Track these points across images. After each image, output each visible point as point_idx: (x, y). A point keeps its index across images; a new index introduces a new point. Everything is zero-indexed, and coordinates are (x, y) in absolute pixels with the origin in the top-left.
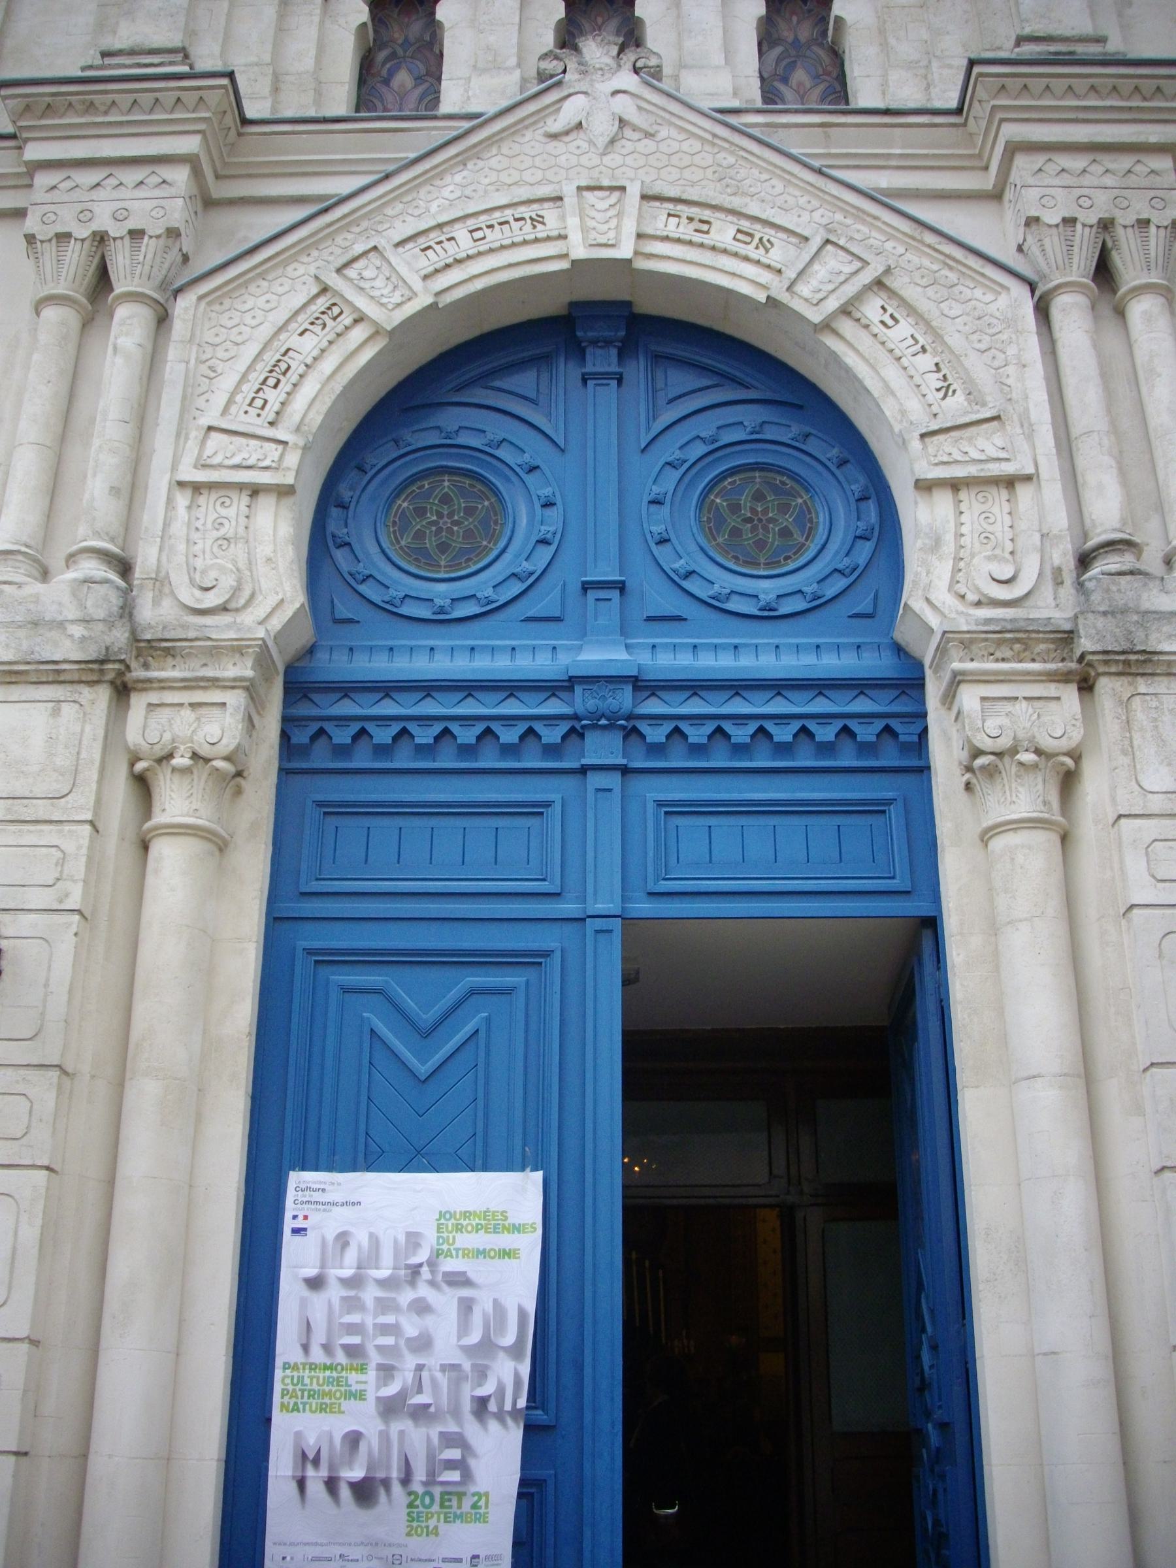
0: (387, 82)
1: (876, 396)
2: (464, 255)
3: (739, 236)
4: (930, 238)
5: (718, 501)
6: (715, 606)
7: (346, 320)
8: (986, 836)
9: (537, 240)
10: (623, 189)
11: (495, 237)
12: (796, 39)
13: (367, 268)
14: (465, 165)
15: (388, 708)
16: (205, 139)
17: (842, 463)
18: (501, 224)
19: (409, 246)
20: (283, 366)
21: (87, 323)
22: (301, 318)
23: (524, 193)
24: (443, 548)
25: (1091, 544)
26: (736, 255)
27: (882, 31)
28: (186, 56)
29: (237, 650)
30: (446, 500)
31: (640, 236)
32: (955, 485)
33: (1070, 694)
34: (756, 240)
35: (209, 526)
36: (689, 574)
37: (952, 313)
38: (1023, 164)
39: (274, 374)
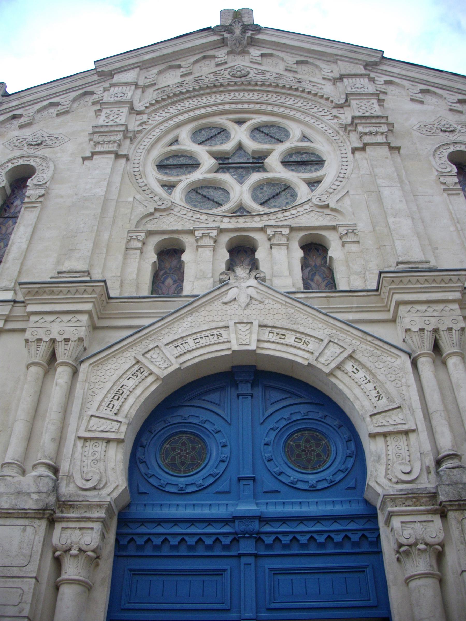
0: (163, 282)
1: (352, 400)
2: (191, 349)
3: (297, 340)
4: (369, 338)
5: (291, 443)
6: (291, 486)
7: (146, 374)
8: (408, 581)
9: (219, 343)
10: (251, 323)
11: (203, 342)
12: (315, 265)
13: (154, 354)
14: (192, 314)
15: (160, 530)
16: (94, 306)
17: (340, 427)
18: (205, 337)
19: (171, 345)
20: (121, 392)
21: (46, 373)
22: (128, 373)
23: (214, 325)
24: (183, 463)
25: (440, 456)
26: (295, 347)
27: (347, 261)
28: (89, 274)
29: (99, 506)
30: (184, 444)
31: (258, 341)
32: (385, 435)
33: (437, 520)
34: (303, 341)
35: (90, 455)
36: (281, 473)
37: (379, 367)
38: (402, 309)
39: (117, 395)
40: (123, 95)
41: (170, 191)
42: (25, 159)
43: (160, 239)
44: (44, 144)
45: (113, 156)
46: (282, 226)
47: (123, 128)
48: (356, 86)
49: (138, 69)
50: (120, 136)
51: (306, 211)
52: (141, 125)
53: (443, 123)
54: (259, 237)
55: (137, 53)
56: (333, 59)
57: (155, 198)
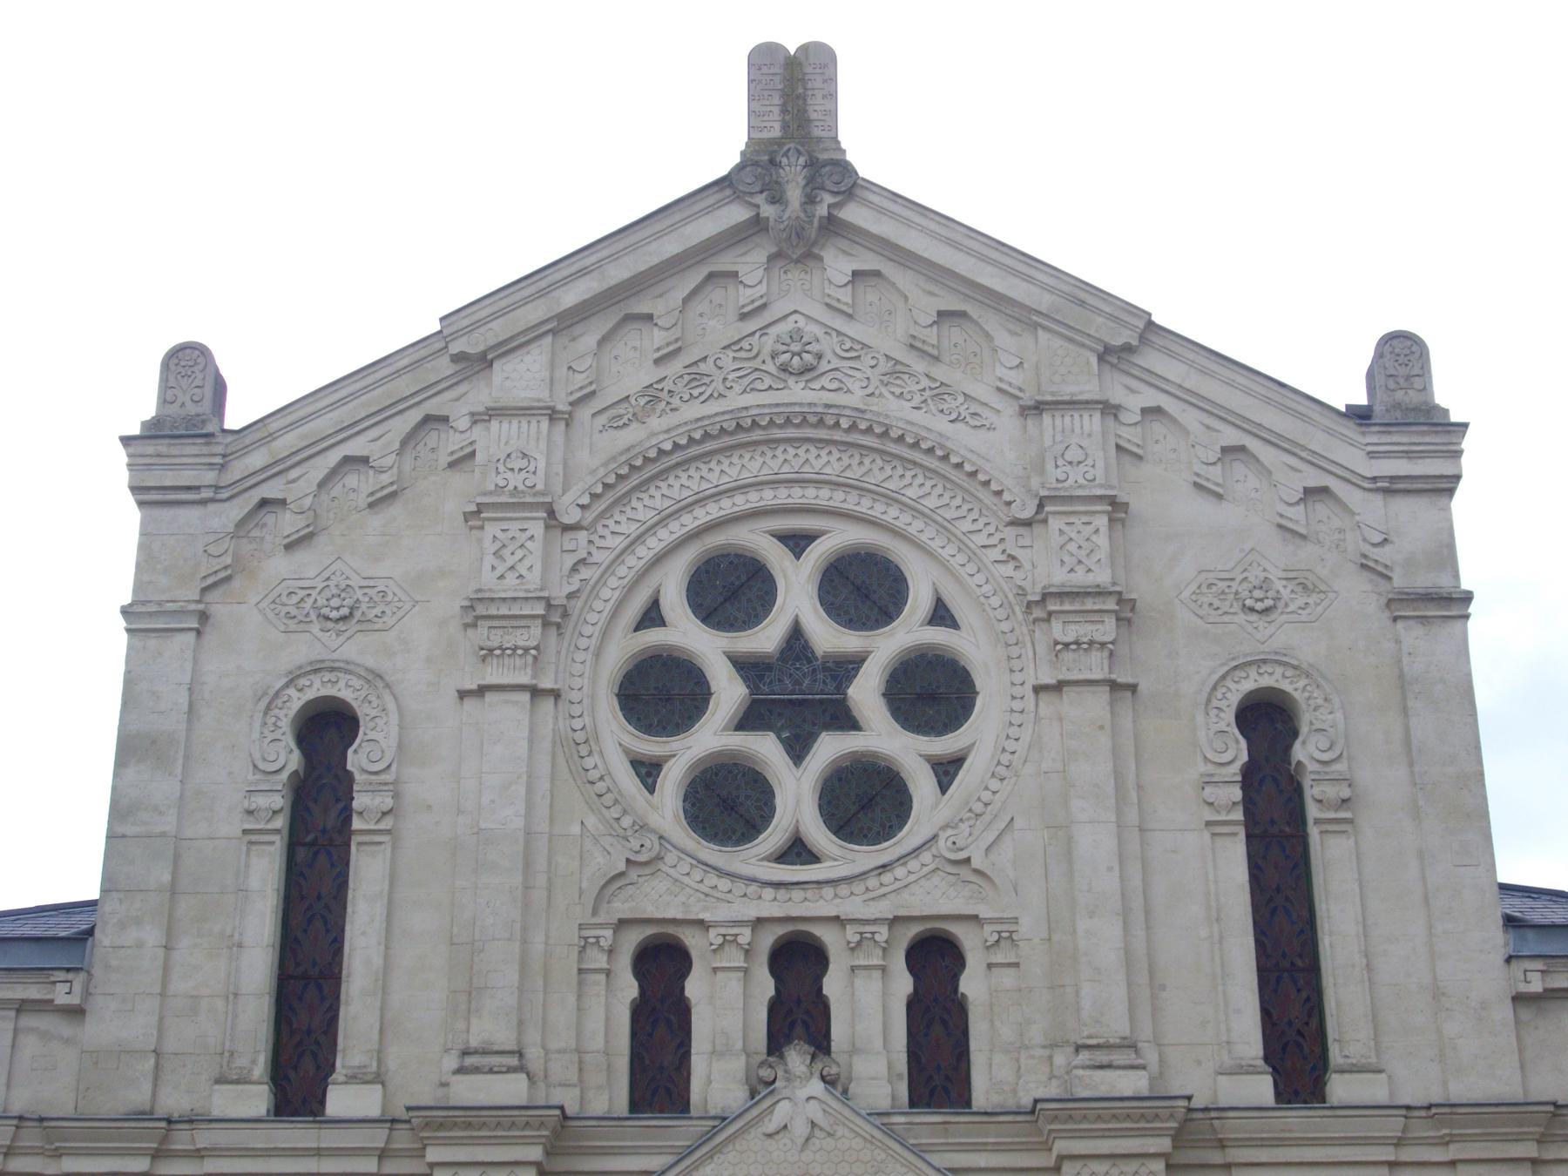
27: (991, 1006)
40: (524, 463)
41: (650, 781)
42: (327, 676)
43: (641, 937)
44: (358, 614)
45: (526, 697)
46: (875, 921)
47: (540, 610)
48: (1068, 456)
49: (549, 339)
50: (536, 630)
51: (926, 870)
52: (574, 570)
53: (1255, 575)
54: (829, 937)
55: (543, 284)
56: (1025, 318)
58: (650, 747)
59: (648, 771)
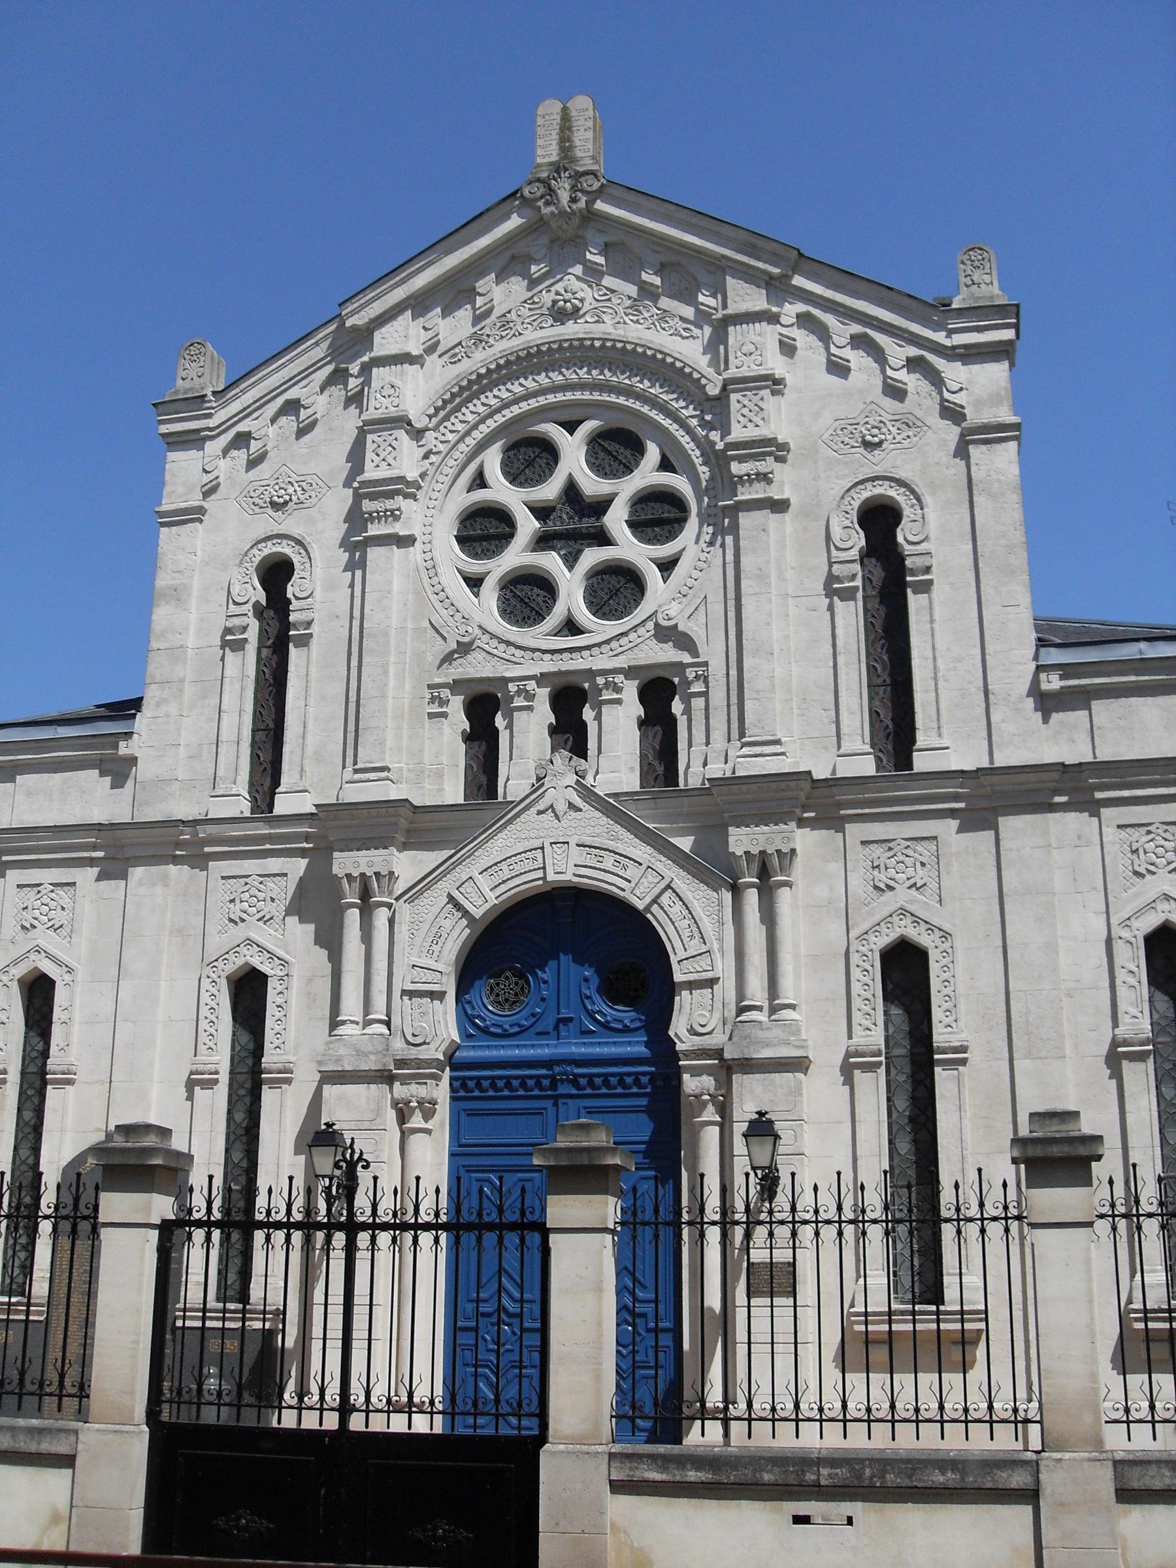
6: (605, 1026)
11: (519, 868)
24: (507, 1000)
48: (745, 349)
57: (458, 616)
58: (475, 566)
59: (474, 582)
